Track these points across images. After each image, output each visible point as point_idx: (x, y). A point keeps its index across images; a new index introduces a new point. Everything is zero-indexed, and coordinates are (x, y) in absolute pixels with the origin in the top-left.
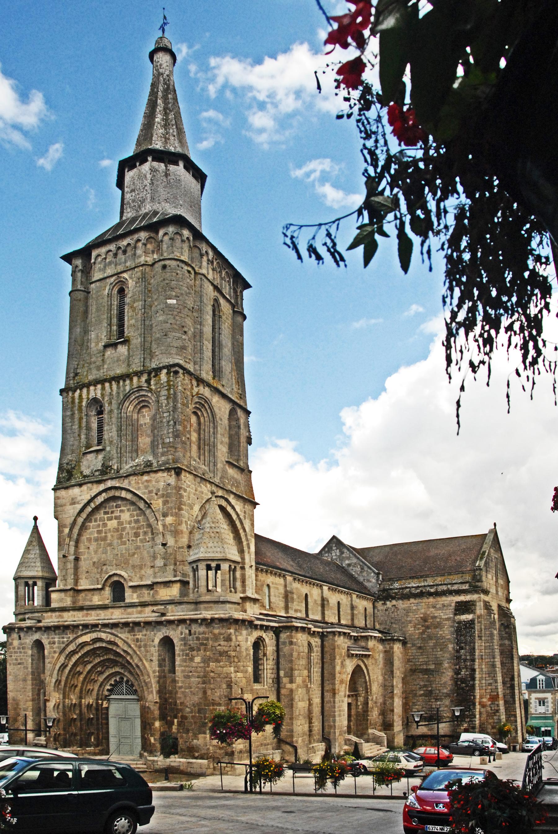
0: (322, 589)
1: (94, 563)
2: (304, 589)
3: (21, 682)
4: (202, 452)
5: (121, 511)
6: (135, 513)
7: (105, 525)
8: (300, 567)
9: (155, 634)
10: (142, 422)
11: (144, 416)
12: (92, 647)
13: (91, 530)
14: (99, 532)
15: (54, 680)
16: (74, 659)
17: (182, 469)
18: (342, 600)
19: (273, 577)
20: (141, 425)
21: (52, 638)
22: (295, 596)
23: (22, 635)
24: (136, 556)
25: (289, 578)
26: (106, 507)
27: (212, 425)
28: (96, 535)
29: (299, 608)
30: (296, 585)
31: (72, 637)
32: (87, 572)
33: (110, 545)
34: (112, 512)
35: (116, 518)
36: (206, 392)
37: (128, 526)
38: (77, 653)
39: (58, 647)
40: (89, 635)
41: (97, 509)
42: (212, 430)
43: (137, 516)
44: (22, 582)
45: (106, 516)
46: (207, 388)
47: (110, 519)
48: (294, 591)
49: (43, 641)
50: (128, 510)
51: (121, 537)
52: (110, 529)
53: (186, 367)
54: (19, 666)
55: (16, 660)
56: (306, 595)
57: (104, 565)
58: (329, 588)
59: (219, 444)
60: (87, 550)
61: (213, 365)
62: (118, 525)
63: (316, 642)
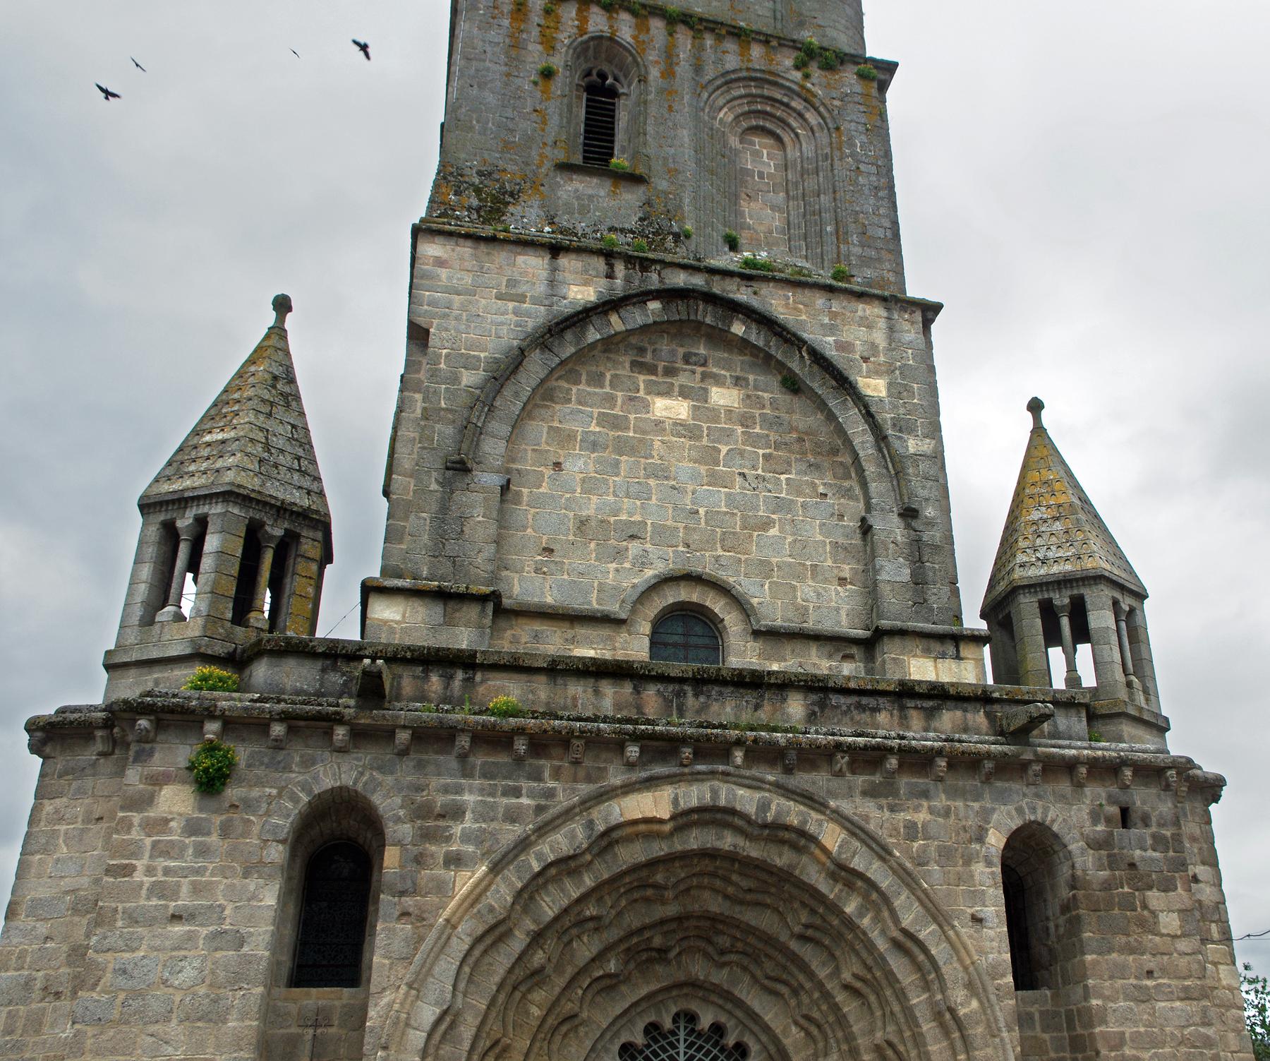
1: (583, 523)
3: (174, 1028)
5: (705, 376)
9: (985, 814)
12: (659, 849)
13: (573, 405)
15: (428, 1014)
16: (549, 905)
21: (446, 790)
24: (774, 532)
26: (642, 351)
28: (594, 428)
31: (565, 795)
32: (549, 551)
33: (661, 473)
35: (685, 393)
37: (740, 430)
38: (574, 873)
39: (475, 838)
40: (667, 793)
41: (610, 344)
49: (377, 799)
50: (738, 382)
51: (710, 456)
54: (178, 929)
55: (159, 890)
57: (633, 537)
60: (548, 472)
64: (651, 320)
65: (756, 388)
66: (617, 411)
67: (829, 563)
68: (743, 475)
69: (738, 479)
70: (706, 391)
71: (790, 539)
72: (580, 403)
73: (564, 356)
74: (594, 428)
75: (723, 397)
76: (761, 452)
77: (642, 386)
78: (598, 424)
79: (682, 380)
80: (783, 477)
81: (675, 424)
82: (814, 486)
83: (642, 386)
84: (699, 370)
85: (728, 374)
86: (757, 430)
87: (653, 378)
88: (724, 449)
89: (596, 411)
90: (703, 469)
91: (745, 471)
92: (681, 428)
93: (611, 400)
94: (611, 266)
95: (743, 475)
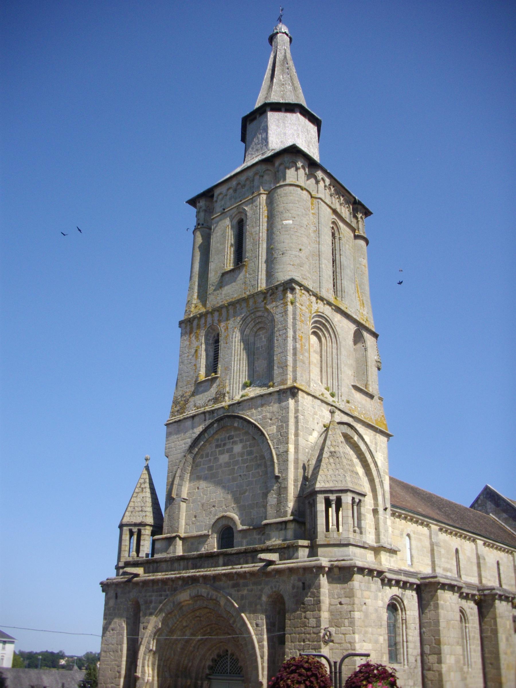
0: (476, 544)
2: (455, 542)
4: (324, 374)
5: (233, 442)
6: (248, 443)
7: (217, 459)
8: (448, 516)
10: (258, 345)
11: (261, 338)
13: (202, 466)
14: (210, 468)
17: (298, 389)
18: (501, 558)
19: (415, 525)
20: (258, 349)
22: (443, 551)
23: (119, 590)
24: (247, 494)
25: (435, 528)
27: (334, 345)
28: (206, 472)
29: (448, 566)
30: (443, 537)
34: (225, 445)
36: (327, 311)
37: (240, 459)
42: (335, 351)
43: (250, 447)
44: (126, 529)
45: (217, 450)
46: (327, 307)
47: (221, 453)
48: (442, 544)
50: (241, 441)
52: (221, 465)
53: (303, 283)
56: (457, 551)
58: (484, 544)
59: (343, 366)
61: (334, 286)
62: (230, 459)
63: (471, 608)
64: (215, 431)
65: (246, 441)
66: (212, 464)
67: (261, 500)
68: (240, 475)
69: (239, 477)
70: (232, 448)
71: (251, 494)
72: (203, 465)
73: (195, 453)
74: (206, 472)
75: (238, 448)
76: (245, 465)
77: (217, 452)
78: (208, 471)
79: (227, 447)
80: (251, 473)
81: (225, 463)
82: (258, 473)
83: (217, 452)
84: (231, 441)
85: (238, 439)
86: (245, 457)
87: (220, 449)
88: (236, 467)
89: (206, 466)
90: (231, 477)
91: (241, 474)
92: (227, 464)
93: (210, 460)
94: (205, 416)
95: (240, 475)
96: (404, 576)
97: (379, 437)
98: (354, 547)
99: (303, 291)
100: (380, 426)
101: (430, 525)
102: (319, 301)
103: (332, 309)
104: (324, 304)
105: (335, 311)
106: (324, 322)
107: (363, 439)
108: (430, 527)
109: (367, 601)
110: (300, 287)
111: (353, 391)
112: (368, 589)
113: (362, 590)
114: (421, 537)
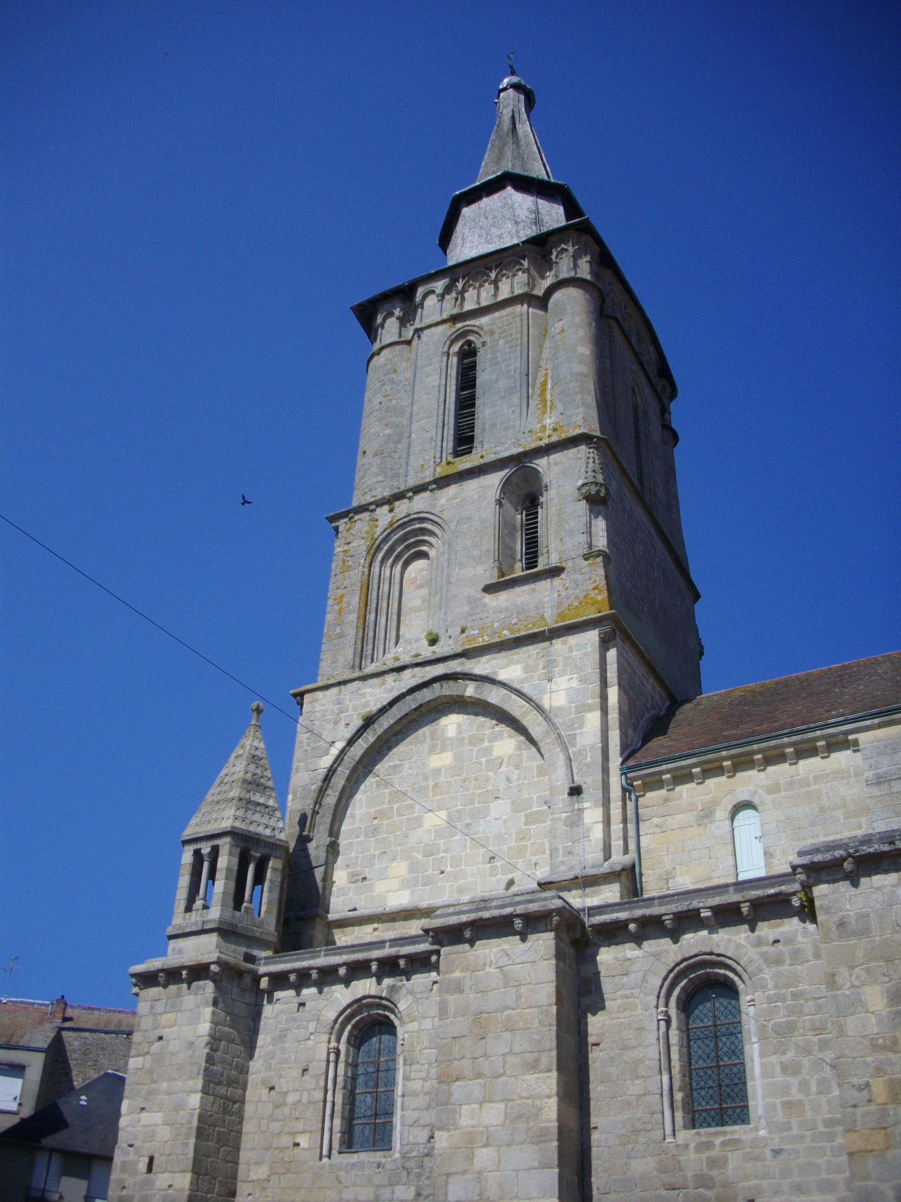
96: (391, 946)
97: (563, 643)
98: (180, 940)
99: (356, 518)
100: (578, 615)
101: (851, 737)
102: (397, 504)
103: (432, 491)
104: (410, 498)
105: (440, 488)
106: (418, 526)
107: (492, 681)
108: (856, 743)
109: (165, 1032)
110: (346, 516)
111: (488, 599)
112: (174, 1008)
113: (155, 1015)
114: (813, 787)
